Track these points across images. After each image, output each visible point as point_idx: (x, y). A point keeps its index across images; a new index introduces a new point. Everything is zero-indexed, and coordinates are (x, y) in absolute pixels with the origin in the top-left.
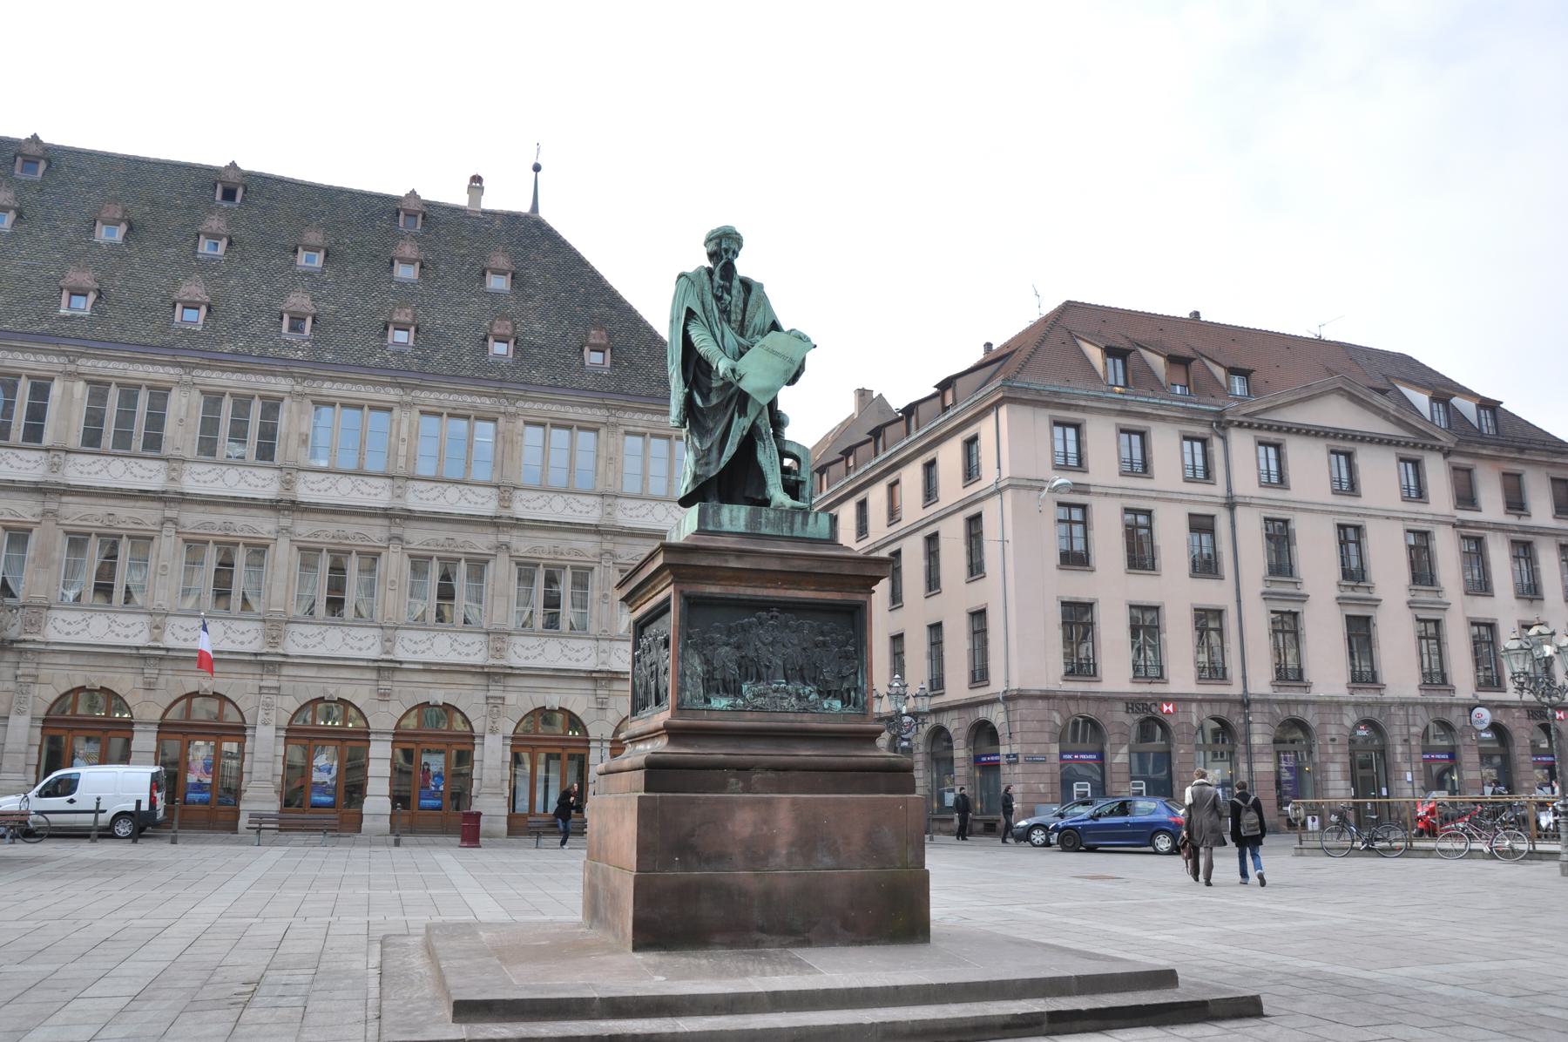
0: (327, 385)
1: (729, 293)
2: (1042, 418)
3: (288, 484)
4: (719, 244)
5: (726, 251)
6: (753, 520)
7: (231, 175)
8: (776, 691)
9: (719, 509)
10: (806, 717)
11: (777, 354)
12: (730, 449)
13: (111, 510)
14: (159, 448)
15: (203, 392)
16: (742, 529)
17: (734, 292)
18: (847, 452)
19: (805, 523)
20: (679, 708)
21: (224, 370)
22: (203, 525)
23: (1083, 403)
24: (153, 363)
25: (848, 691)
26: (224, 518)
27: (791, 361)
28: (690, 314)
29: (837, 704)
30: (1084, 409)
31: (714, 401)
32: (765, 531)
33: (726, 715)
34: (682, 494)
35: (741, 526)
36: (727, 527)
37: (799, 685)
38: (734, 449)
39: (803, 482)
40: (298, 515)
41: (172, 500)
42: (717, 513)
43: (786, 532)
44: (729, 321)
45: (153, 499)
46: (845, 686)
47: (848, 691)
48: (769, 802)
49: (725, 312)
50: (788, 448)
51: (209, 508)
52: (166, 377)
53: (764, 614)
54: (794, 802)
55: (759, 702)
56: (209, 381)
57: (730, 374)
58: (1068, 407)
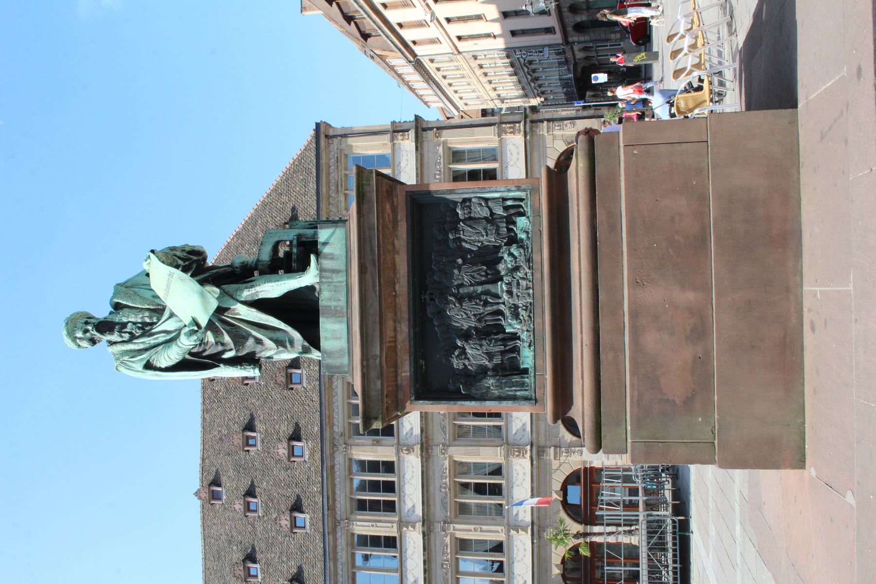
0: (336, 429)
1: (127, 323)
3: (410, 449)
5: (86, 331)
6: (335, 314)
7: (203, 495)
8: (510, 293)
10: (536, 257)
11: (168, 287)
13: (439, 566)
14: (394, 538)
15: (352, 513)
16: (344, 326)
17: (125, 320)
18: (349, 19)
19: (331, 257)
21: (334, 500)
22: (444, 504)
24: (335, 547)
25: (506, 208)
26: (437, 492)
27: (171, 275)
28: (149, 366)
29: (522, 222)
31: (227, 339)
32: (343, 303)
33: (538, 351)
35: (340, 327)
36: (343, 343)
37: (501, 267)
39: (299, 236)
40: (430, 443)
41: (429, 528)
43: (342, 278)
44: (152, 324)
45: (429, 539)
46: (499, 211)
47: (506, 208)
48: (635, 315)
49: (146, 329)
50: (266, 256)
51: (431, 502)
52: (343, 537)
53: (430, 310)
54: (635, 284)
56: (343, 510)
57: (195, 337)
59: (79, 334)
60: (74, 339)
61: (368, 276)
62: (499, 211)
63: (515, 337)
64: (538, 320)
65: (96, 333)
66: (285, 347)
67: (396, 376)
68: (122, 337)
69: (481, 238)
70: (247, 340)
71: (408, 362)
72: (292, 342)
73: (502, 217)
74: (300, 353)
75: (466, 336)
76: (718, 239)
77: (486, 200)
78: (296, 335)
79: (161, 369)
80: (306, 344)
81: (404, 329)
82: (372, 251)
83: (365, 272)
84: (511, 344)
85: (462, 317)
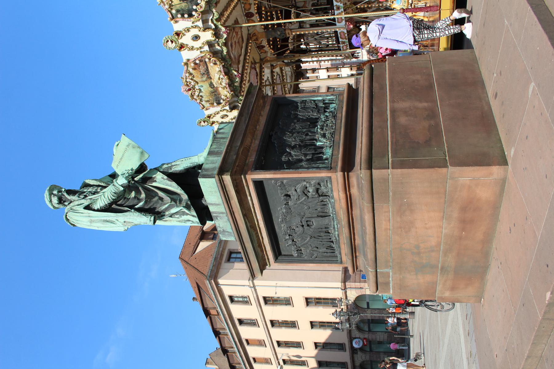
1: (84, 192)
2: (225, 265)
4: (55, 195)
8: (322, 129)
9: (204, 169)
10: (339, 115)
12: (174, 187)
20: (330, 168)
23: (221, 249)
28: (88, 208)
29: (332, 106)
30: (224, 249)
31: (143, 195)
34: (196, 220)
38: (174, 184)
42: (207, 170)
46: (321, 105)
47: (324, 104)
55: (328, 135)
58: (222, 255)
59: (55, 192)
60: (51, 194)
61: (243, 118)
62: (321, 105)
63: (321, 147)
64: (337, 137)
65: (65, 194)
66: (176, 203)
67: (246, 160)
68: (79, 197)
69: (309, 114)
70: (154, 197)
71: (255, 155)
72: (181, 201)
73: (322, 107)
74: (183, 207)
75: (293, 148)
76: (439, 85)
77: (314, 101)
78: (185, 197)
79: (94, 210)
80: (189, 203)
81: (256, 143)
82: (249, 110)
83: (242, 116)
84: (319, 151)
85: (291, 140)
